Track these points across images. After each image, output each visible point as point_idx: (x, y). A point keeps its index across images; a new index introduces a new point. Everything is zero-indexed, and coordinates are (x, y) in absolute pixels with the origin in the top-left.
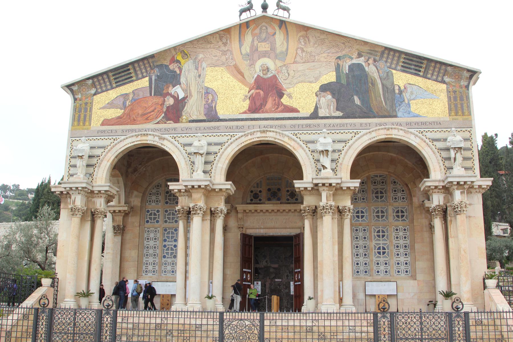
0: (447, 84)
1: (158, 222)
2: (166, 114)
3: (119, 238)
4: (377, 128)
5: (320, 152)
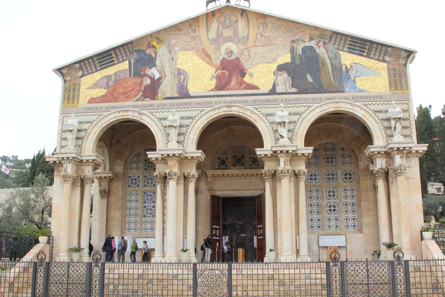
0: (387, 63)
1: (138, 186)
2: (144, 93)
3: (105, 201)
4: (327, 102)
5: (278, 124)
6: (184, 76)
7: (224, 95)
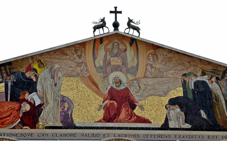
2: (21, 118)
6: (69, 105)
7: (112, 127)
